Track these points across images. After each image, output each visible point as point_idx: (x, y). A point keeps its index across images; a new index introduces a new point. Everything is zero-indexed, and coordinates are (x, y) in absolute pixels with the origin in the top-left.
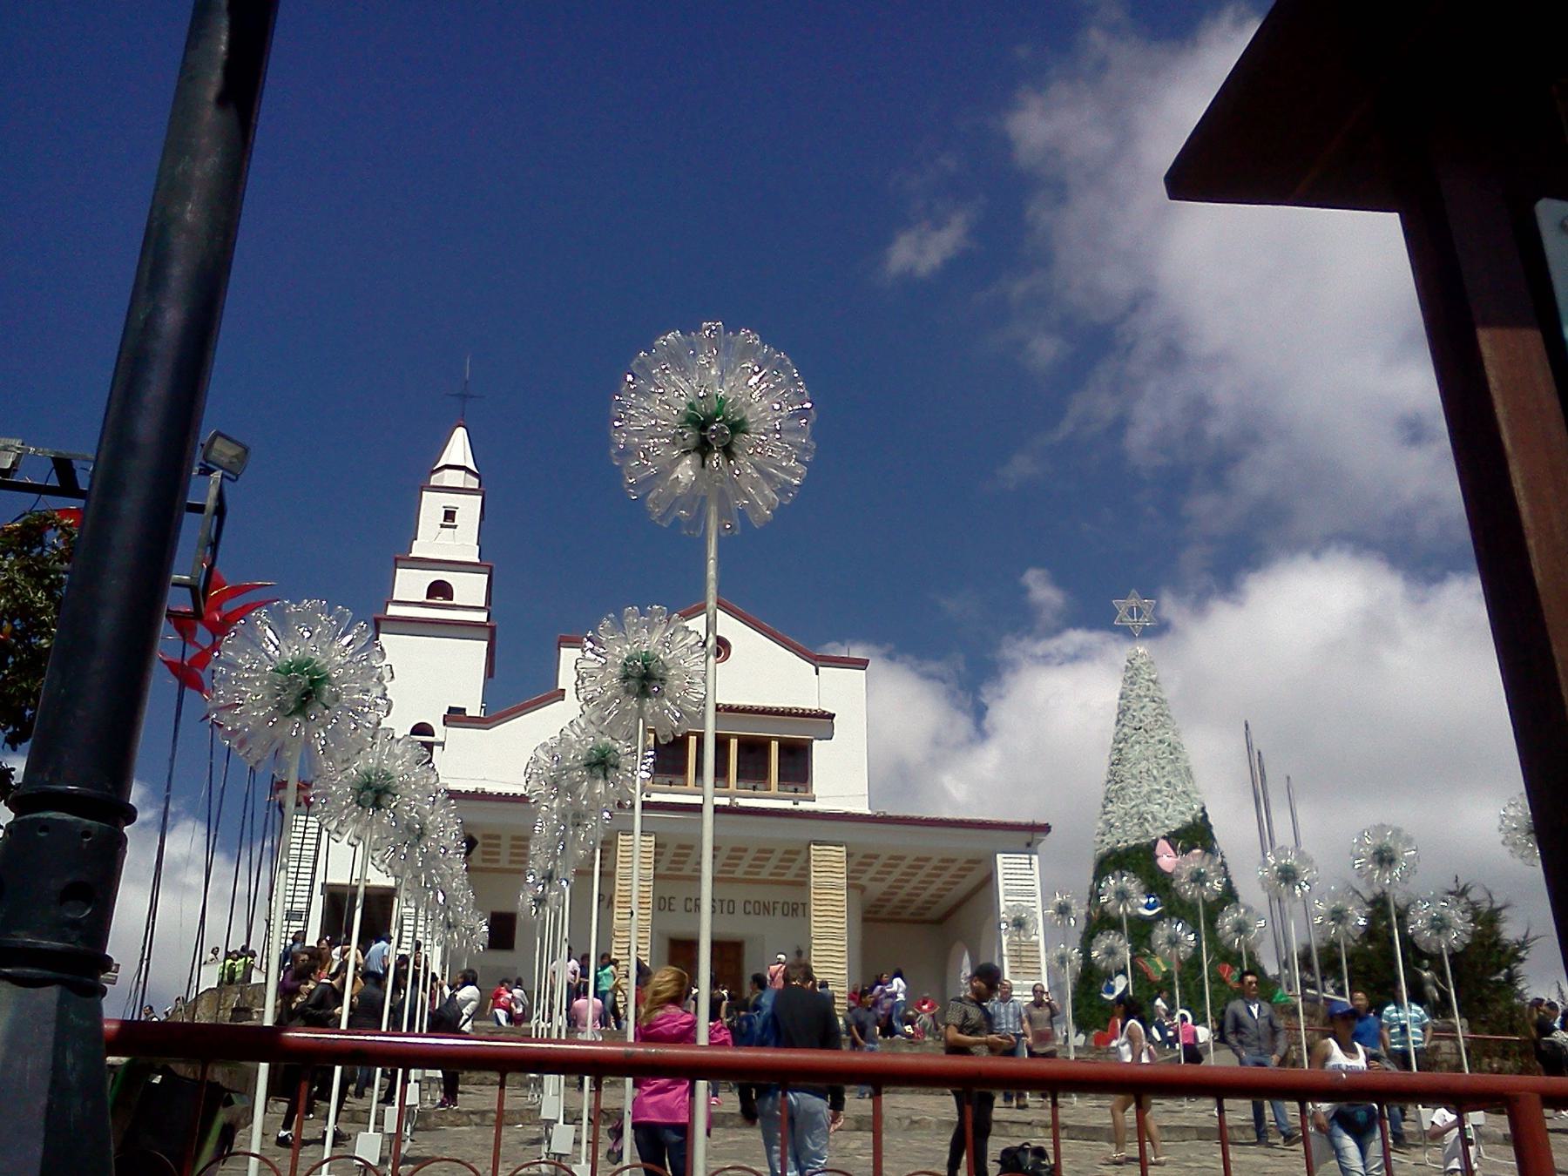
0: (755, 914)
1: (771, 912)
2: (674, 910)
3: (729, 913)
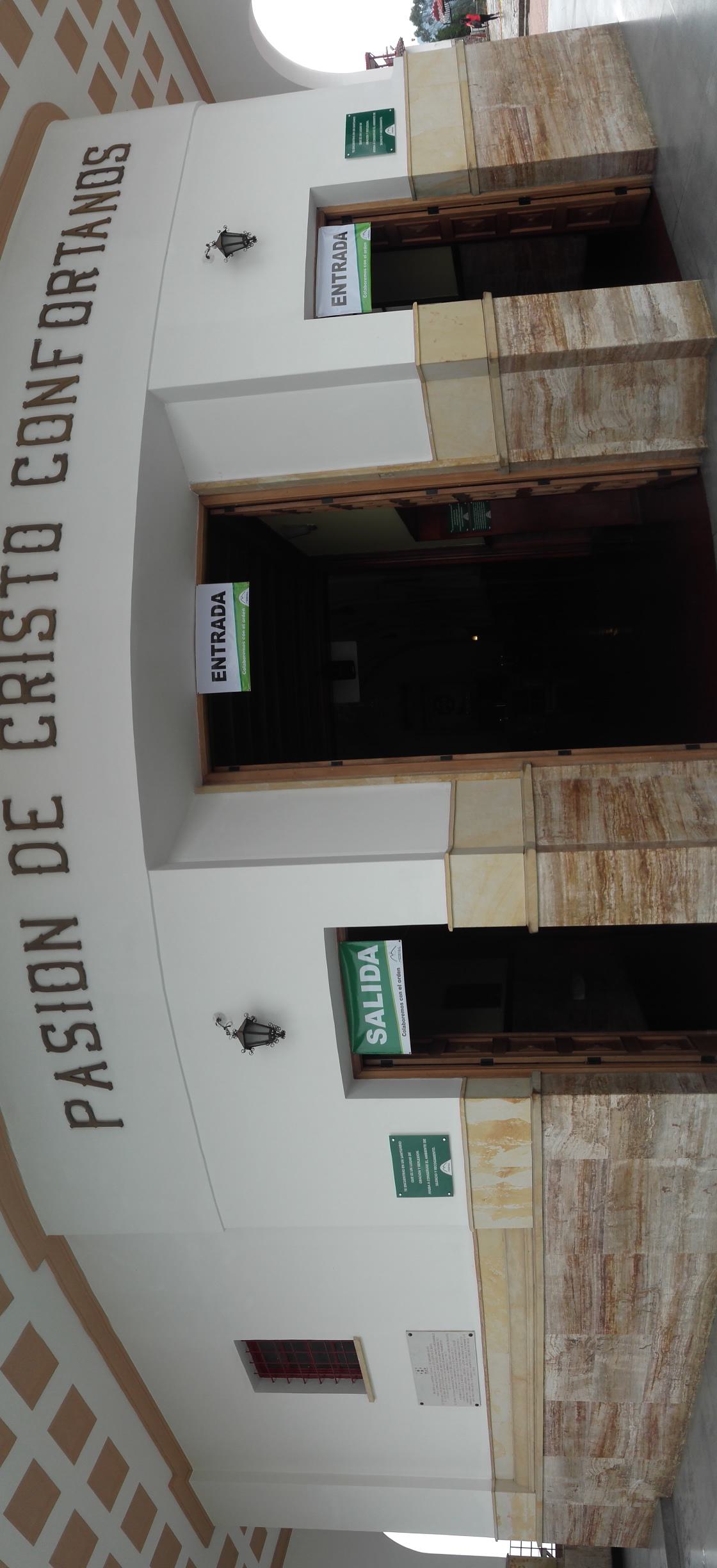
0: (66, 436)
2: (57, 800)
3: (55, 547)
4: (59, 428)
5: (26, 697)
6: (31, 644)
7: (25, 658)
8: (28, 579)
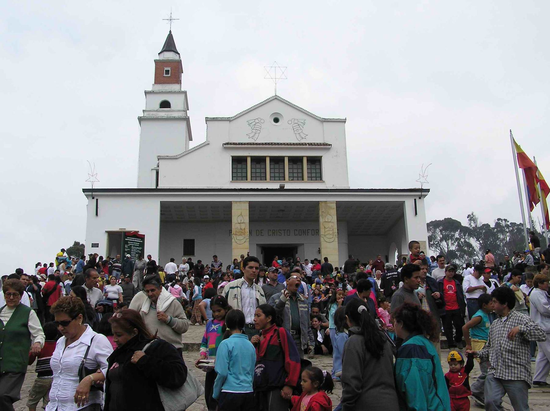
1: (307, 234)
4: (300, 234)
5: (273, 233)
6: (278, 233)
7: (277, 232)
8: (284, 233)
